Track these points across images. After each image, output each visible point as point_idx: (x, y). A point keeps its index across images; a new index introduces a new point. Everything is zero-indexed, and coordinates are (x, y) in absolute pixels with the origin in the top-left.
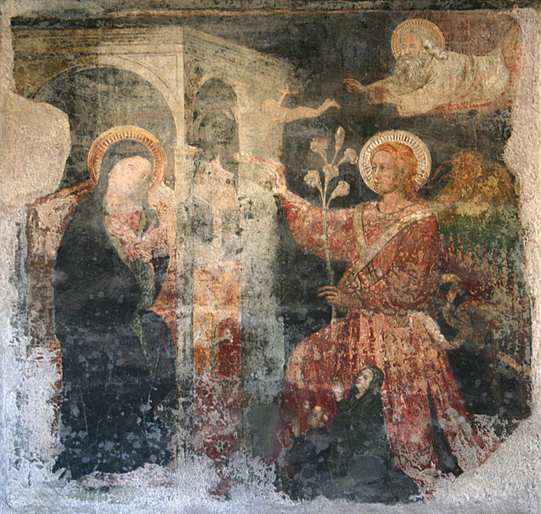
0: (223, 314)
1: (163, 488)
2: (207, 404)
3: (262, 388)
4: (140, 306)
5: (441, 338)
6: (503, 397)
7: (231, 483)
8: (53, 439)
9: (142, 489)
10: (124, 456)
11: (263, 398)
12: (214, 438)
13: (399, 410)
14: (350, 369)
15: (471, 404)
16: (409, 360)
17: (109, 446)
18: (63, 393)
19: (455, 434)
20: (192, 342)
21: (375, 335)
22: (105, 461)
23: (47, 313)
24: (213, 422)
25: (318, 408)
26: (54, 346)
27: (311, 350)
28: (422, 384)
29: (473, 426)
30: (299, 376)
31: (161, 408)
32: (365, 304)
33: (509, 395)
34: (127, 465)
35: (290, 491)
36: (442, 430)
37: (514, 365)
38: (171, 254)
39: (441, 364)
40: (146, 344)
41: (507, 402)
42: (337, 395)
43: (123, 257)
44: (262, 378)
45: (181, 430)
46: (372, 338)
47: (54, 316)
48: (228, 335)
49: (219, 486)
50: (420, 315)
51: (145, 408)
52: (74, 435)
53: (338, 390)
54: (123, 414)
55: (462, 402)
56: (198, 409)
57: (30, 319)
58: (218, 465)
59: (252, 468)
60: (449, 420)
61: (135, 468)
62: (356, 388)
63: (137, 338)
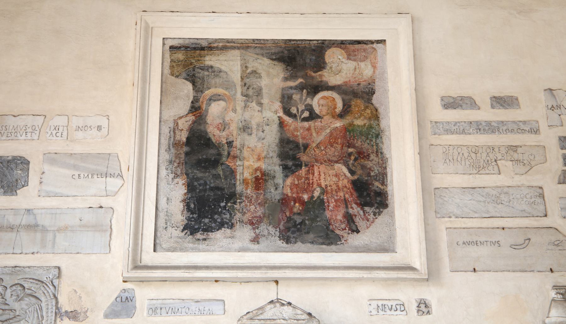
0: (256, 165)
1: (230, 239)
2: (249, 203)
3: (273, 196)
4: (221, 162)
5: (349, 175)
6: (376, 200)
7: (259, 237)
8: (182, 218)
9: (221, 239)
10: (213, 225)
11: (273, 200)
12: (252, 217)
13: (332, 205)
14: (311, 188)
15: (362, 203)
16: (336, 184)
17: (207, 220)
18: (187, 198)
19: (356, 215)
20: (243, 177)
21: (321, 174)
22: (205, 227)
23: (181, 164)
24: (252, 210)
25: (297, 204)
26: (184, 178)
27: (294, 180)
28: (341, 194)
29: (364, 212)
30: (289, 191)
31: (229, 204)
32: (317, 161)
33: (379, 199)
34: (214, 229)
35: (285, 240)
36: (351, 214)
37: (380, 186)
38: (234, 140)
39: (349, 186)
40: (223, 177)
41: (378, 201)
42: (305, 199)
43: (214, 141)
44: (273, 191)
45: (238, 214)
46: (320, 175)
47: (184, 166)
48: (258, 174)
49: (255, 238)
50: (340, 165)
51: (223, 204)
52: (191, 216)
53: (306, 197)
54: (213, 207)
55: (359, 202)
56: (246, 205)
57: (174, 167)
58: (254, 229)
59: (269, 230)
60: (353, 209)
61: (218, 230)
62: (313, 196)
63: (219, 175)
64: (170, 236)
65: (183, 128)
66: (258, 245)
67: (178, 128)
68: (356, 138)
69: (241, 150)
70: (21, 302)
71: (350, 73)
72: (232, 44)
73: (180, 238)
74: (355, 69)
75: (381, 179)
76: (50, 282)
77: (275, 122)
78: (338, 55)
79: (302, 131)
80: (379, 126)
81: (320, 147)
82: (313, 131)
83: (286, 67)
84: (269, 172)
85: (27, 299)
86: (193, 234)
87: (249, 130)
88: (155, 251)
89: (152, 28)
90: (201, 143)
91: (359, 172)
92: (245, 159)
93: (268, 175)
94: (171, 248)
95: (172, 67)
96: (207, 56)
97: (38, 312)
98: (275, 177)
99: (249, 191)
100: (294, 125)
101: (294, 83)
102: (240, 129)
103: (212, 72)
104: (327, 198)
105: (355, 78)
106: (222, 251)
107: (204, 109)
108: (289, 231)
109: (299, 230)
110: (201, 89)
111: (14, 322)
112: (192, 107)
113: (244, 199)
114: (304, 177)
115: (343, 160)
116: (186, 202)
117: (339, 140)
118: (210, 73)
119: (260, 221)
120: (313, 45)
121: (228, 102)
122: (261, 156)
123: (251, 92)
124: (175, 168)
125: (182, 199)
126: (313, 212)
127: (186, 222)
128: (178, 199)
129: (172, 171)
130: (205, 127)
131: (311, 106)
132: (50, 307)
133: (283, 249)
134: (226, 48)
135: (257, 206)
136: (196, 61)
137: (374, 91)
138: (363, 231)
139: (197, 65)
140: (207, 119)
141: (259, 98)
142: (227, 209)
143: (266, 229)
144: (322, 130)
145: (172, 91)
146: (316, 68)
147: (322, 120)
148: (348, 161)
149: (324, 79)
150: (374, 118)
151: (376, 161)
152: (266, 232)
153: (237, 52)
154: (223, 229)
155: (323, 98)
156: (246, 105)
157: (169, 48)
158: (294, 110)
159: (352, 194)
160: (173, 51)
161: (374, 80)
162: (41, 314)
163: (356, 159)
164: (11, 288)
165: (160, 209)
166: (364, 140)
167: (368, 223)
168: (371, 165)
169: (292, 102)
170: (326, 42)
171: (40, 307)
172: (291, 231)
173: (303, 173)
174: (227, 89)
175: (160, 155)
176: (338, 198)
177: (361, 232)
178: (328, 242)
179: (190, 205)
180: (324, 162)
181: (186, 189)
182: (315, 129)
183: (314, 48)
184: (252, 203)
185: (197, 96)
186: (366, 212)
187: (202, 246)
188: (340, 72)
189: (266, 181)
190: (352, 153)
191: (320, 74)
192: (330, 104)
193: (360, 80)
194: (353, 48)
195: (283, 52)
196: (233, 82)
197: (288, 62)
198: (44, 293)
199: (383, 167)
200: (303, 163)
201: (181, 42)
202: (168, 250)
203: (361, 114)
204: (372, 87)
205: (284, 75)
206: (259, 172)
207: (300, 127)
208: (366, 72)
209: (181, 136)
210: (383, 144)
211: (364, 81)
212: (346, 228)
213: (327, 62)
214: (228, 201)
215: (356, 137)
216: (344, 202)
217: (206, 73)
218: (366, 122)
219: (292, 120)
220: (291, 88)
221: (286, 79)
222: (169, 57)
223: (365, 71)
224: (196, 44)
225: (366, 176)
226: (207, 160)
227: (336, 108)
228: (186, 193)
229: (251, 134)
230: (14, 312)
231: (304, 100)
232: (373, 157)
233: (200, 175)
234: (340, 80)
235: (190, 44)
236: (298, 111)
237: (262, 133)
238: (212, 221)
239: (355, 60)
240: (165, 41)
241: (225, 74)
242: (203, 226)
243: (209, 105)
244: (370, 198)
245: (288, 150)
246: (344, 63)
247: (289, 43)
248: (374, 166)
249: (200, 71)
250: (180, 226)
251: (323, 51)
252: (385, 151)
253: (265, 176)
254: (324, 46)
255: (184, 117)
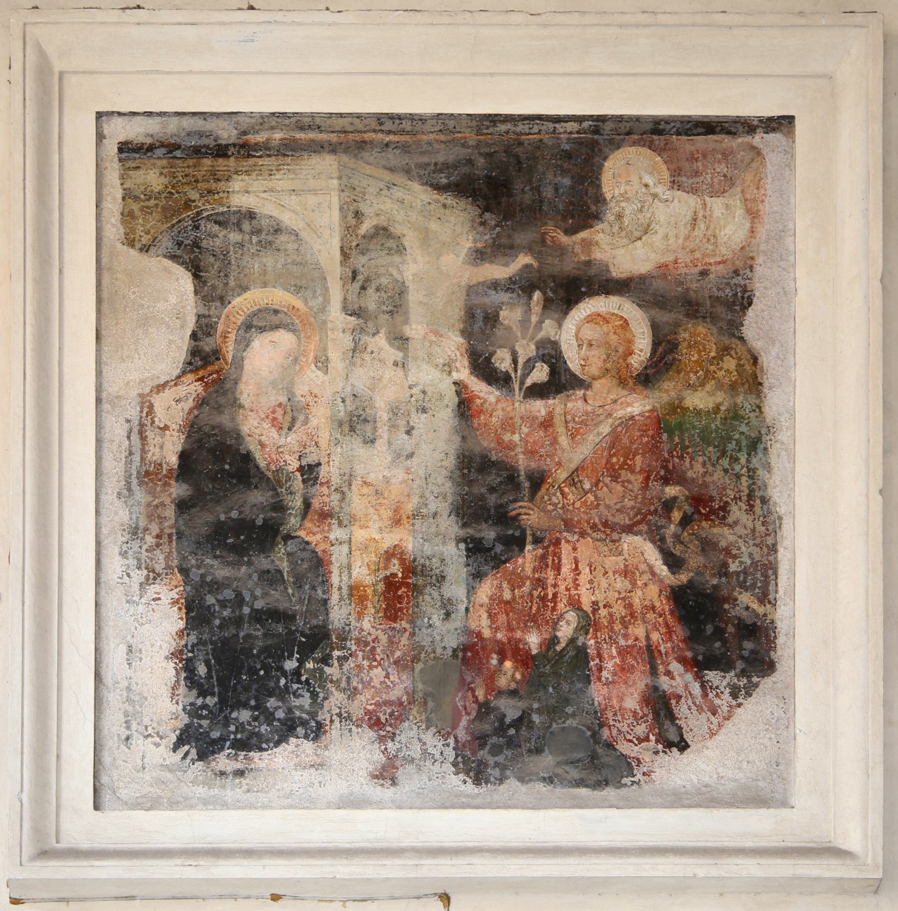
0: (389, 540)
1: (312, 770)
2: (368, 659)
3: (438, 638)
4: (284, 530)
5: (663, 570)
6: (741, 648)
7: (398, 764)
8: (173, 708)
9: (286, 772)
10: (264, 729)
11: (439, 651)
12: (377, 704)
13: (609, 665)
14: (549, 612)
15: (700, 658)
16: (623, 599)
17: (245, 715)
18: (186, 645)
19: (681, 697)
20: (350, 577)
21: (580, 567)
22: (239, 736)
23: (165, 539)
24: (376, 682)
25: (508, 664)
26: (174, 583)
28: (639, 631)
29: (703, 687)
30: (485, 622)
31: (310, 665)
32: (569, 525)
33: (748, 645)
34: (268, 741)
35: (472, 774)
36: (664, 692)
37: (755, 606)
38: (323, 460)
39: (663, 605)
41: (746, 653)
43: (262, 464)
45: (336, 693)
46: (576, 570)
47: (174, 543)
48: (395, 568)
49: (384, 768)
50: (638, 539)
52: (199, 702)
53: (533, 640)
54: (262, 673)
55: (689, 654)
56: (358, 666)
57: (145, 547)
58: (382, 739)
59: (425, 744)
60: (673, 678)
61: (277, 744)
62: (556, 637)
63: (280, 572)
64: (140, 763)
65: (169, 423)
66: (392, 788)
67: (153, 422)
68: (688, 453)
69: (343, 493)
71: (677, 237)
72: (312, 135)
73: (169, 769)
74: (695, 220)
75: (759, 585)
77: (446, 402)
78: (642, 173)
79: (525, 430)
80: (761, 412)
81: (581, 481)
82: (561, 429)
83: (481, 216)
84: (427, 563)
86: (207, 758)
87: (368, 428)
88: (96, 807)
89: (61, 74)
90: (223, 470)
91: (695, 560)
92: (355, 521)
93: (424, 571)
94: (145, 800)
95: (128, 216)
96: (235, 176)
98: (444, 577)
99: (366, 625)
100: (503, 409)
101: (506, 269)
102: (341, 424)
103: (252, 233)
104: (597, 642)
105: (692, 252)
106: (290, 807)
107: (230, 358)
108: (482, 746)
109: (511, 743)
110: (219, 292)
112: (195, 352)
113: (354, 648)
114: (529, 578)
115: (648, 523)
116: (185, 657)
117: (639, 459)
118: (247, 237)
119: (401, 715)
120: (566, 136)
121: (302, 335)
122: (402, 511)
123: (371, 300)
124: (147, 551)
125: (172, 650)
126: (554, 688)
127: (186, 719)
128: (161, 648)
129: (139, 560)
130: (233, 419)
131: (555, 345)
133: (464, 800)
134: (292, 150)
135: (390, 670)
136: (202, 196)
137: (749, 297)
138: (700, 745)
139: (206, 210)
140: (241, 393)
141: (399, 318)
142: (303, 678)
143: (415, 740)
144: (586, 425)
145: (132, 297)
146: (573, 217)
147: (589, 393)
148: (662, 527)
149: (598, 255)
150: (746, 386)
151: (745, 527)
152: (415, 751)
153: (327, 163)
154: (292, 740)
155: (592, 319)
156: (356, 343)
157: (116, 150)
158: (502, 361)
159: (670, 632)
160: (128, 159)
161: (752, 258)
163: (685, 521)
165: (108, 679)
166: (714, 458)
167: (713, 719)
168: (732, 538)
169: (499, 332)
170: (608, 127)
172: (488, 747)
173: (527, 565)
174: (298, 289)
175: (103, 511)
176: (630, 642)
177: (693, 747)
178: (594, 777)
179: (195, 669)
180: (589, 531)
181: (181, 619)
182: (566, 422)
183: (567, 147)
184: (375, 660)
185: (207, 313)
186: (711, 688)
187: (233, 791)
188: (646, 233)
189: (417, 590)
190: (675, 498)
191: (583, 240)
192: (613, 339)
193: (707, 260)
194: (689, 148)
195: (470, 162)
196: (318, 267)
197: (486, 198)
199: (767, 546)
200: (529, 532)
201: (153, 127)
202: (137, 805)
203: (707, 371)
204: (743, 283)
205: (475, 241)
206: (396, 561)
207: (522, 418)
208: (726, 231)
209: (161, 447)
210: (769, 472)
211: (720, 263)
212: (648, 734)
213: (608, 196)
214: (306, 652)
215: (690, 450)
216: (646, 656)
217: (235, 237)
218: (720, 400)
219: (498, 393)
220: (495, 285)
221: (480, 256)
222: (118, 182)
223: (725, 227)
224: (201, 134)
225: (714, 575)
226: (243, 526)
227: (631, 353)
228: (182, 631)
229: (373, 441)
231: (536, 326)
232: (737, 512)
233: (222, 572)
234: (648, 260)
235: (183, 134)
236: (515, 361)
237: (406, 437)
238: (262, 718)
239: (693, 191)
240: (105, 126)
241: (293, 238)
242: (235, 733)
243: (244, 344)
244: (724, 642)
245: (483, 490)
246: (660, 200)
247: (491, 130)
248: (741, 543)
249: (216, 228)
250: (169, 733)
251: (597, 159)
252: (776, 493)
253: (415, 573)
254: (601, 142)
255: (171, 387)
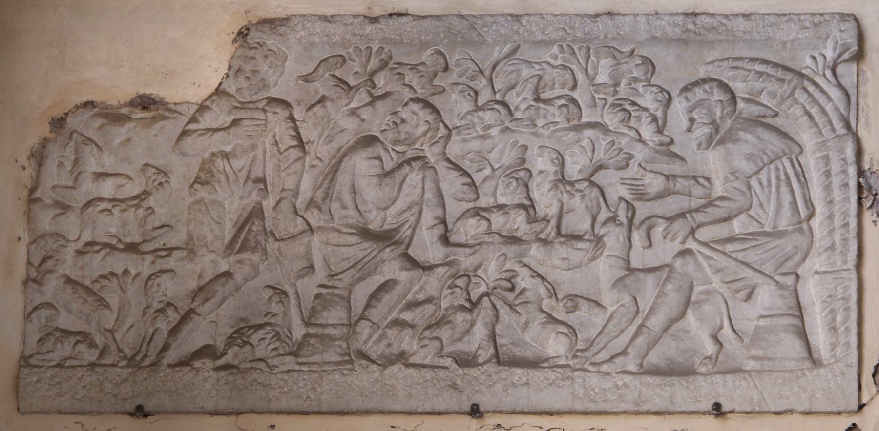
70: (730, 145)
76: (829, 74)
85: (749, 137)
97: (792, 187)
111: (709, 223)
132: (835, 167)
162: (804, 196)
164: (689, 95)
171: (799, 169)
198: (811, 117)
230: (706, 184)
